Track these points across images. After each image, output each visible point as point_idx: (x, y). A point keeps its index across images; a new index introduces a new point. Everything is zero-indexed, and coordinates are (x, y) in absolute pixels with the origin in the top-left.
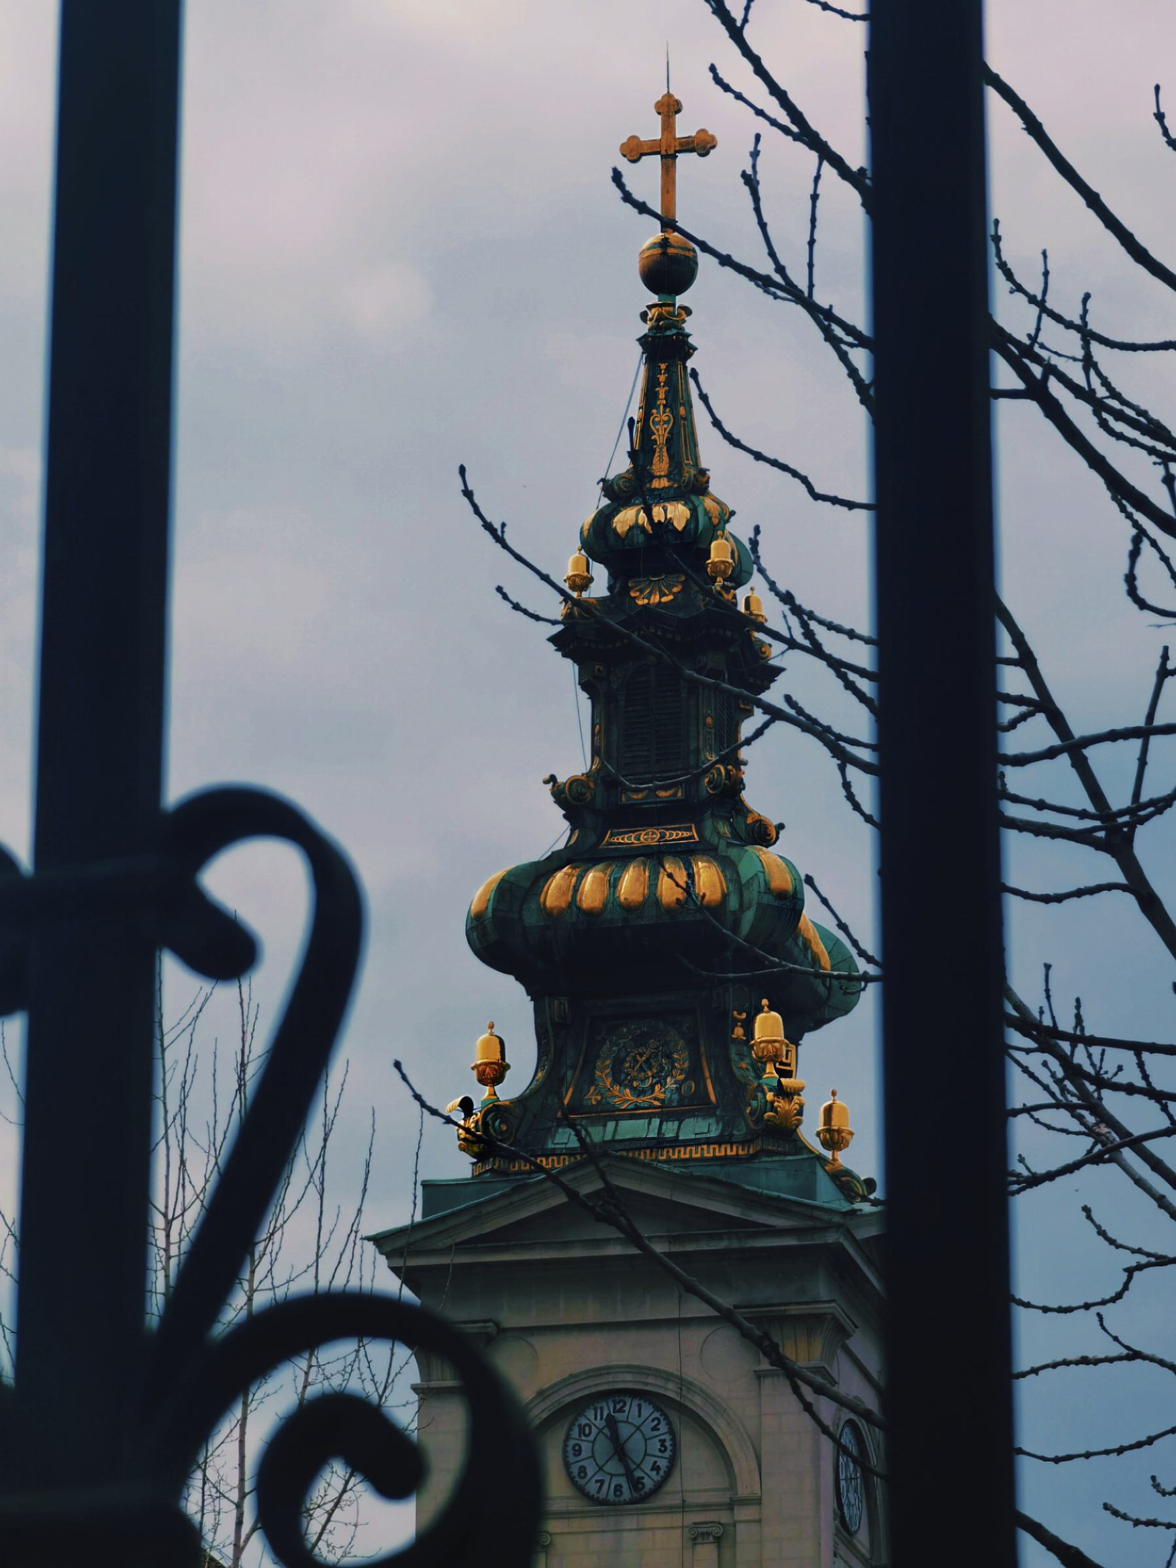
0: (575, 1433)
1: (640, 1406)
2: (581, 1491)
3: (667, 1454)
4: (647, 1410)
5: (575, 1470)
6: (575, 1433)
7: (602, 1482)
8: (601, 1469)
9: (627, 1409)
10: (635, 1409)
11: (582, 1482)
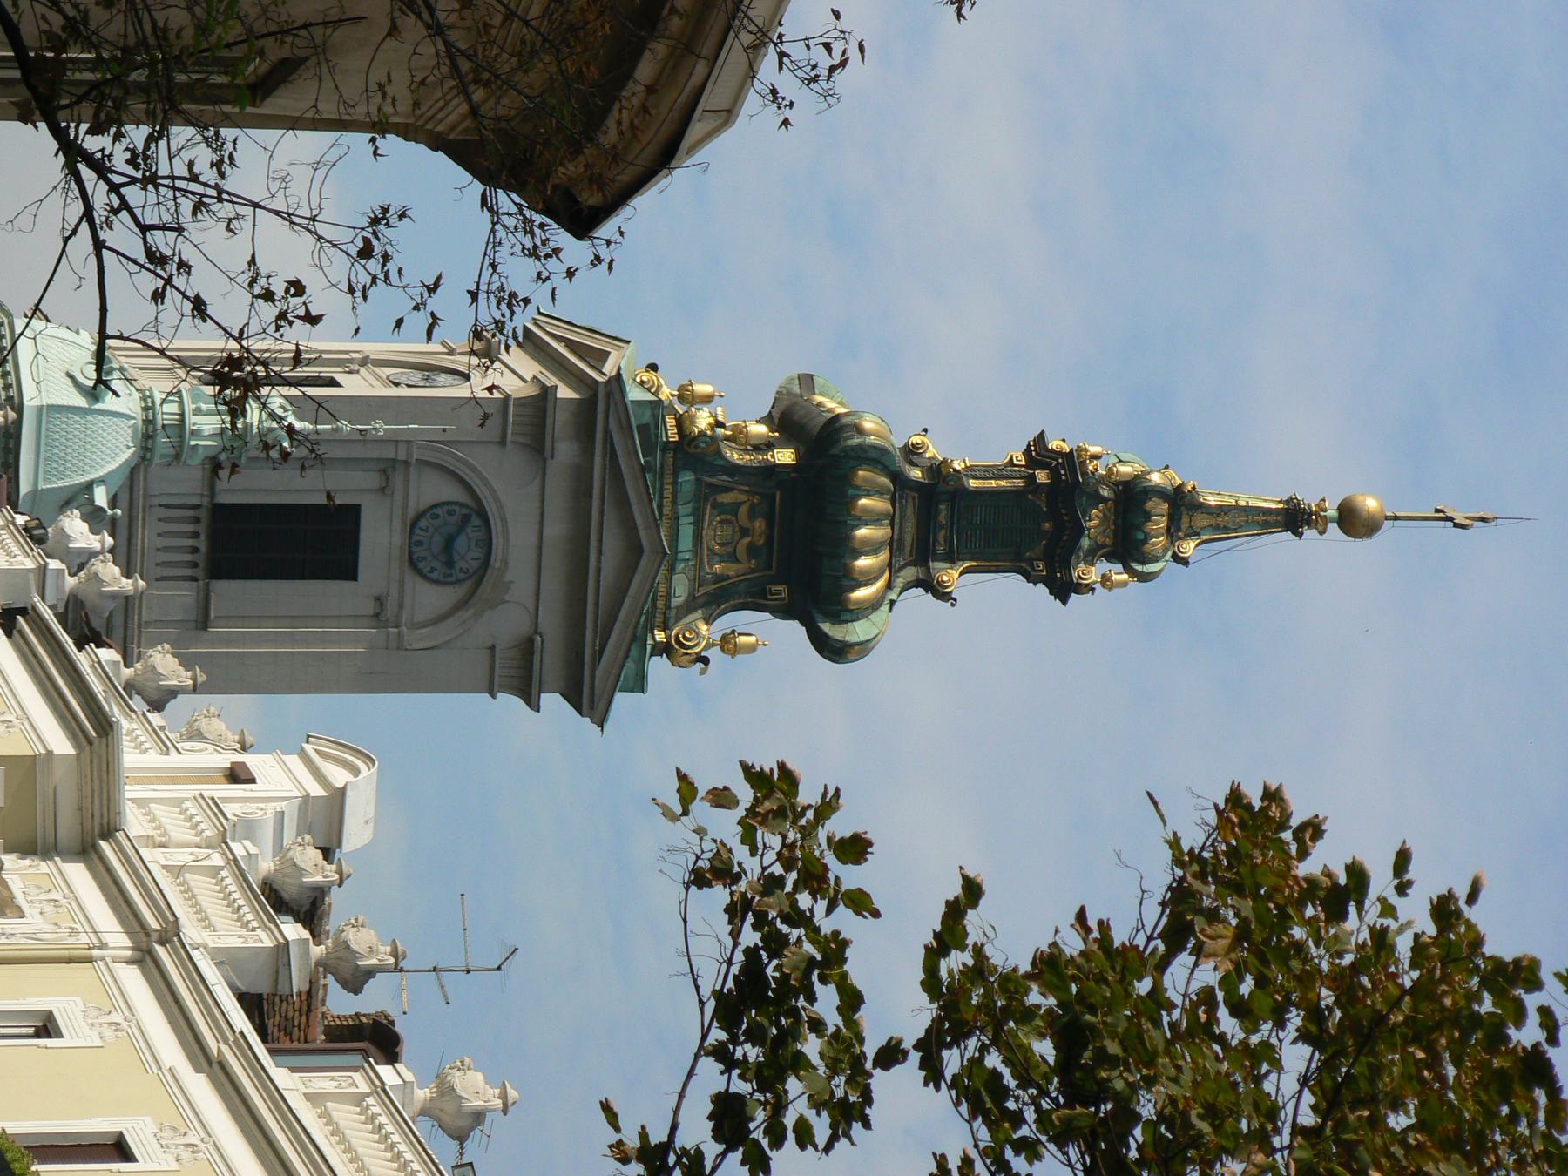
0: (464, 511)
2: (420, 516)
3: (442, 579)
4: (475, 564)
5: (438, 511)
7: (426, 531)
8: (436, 530)
9: (479, 549)
10: (476, 555)
11: (428, 515)
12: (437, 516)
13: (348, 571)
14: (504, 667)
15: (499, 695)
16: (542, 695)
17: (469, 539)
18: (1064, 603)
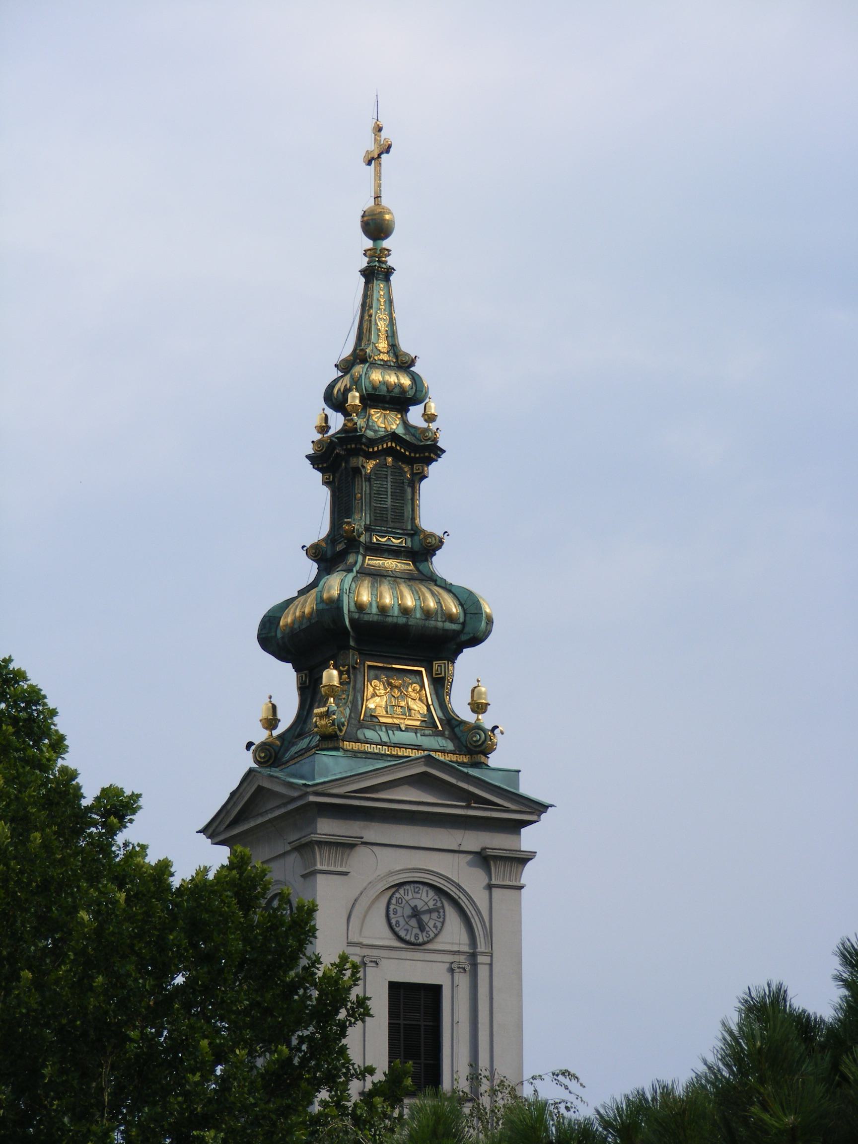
1: (427, 891)
3: (441, 920)
4: (431, 893)
5: (393, 922)
6: (394, 901)
10: (424, 894)
11: (397, 929)
12: (397, 922)
13: (436, 990)
14: (503, 878)
15: (523, 881)
16: (522, 849)
17: (413, 898)
18: (443, 451)
